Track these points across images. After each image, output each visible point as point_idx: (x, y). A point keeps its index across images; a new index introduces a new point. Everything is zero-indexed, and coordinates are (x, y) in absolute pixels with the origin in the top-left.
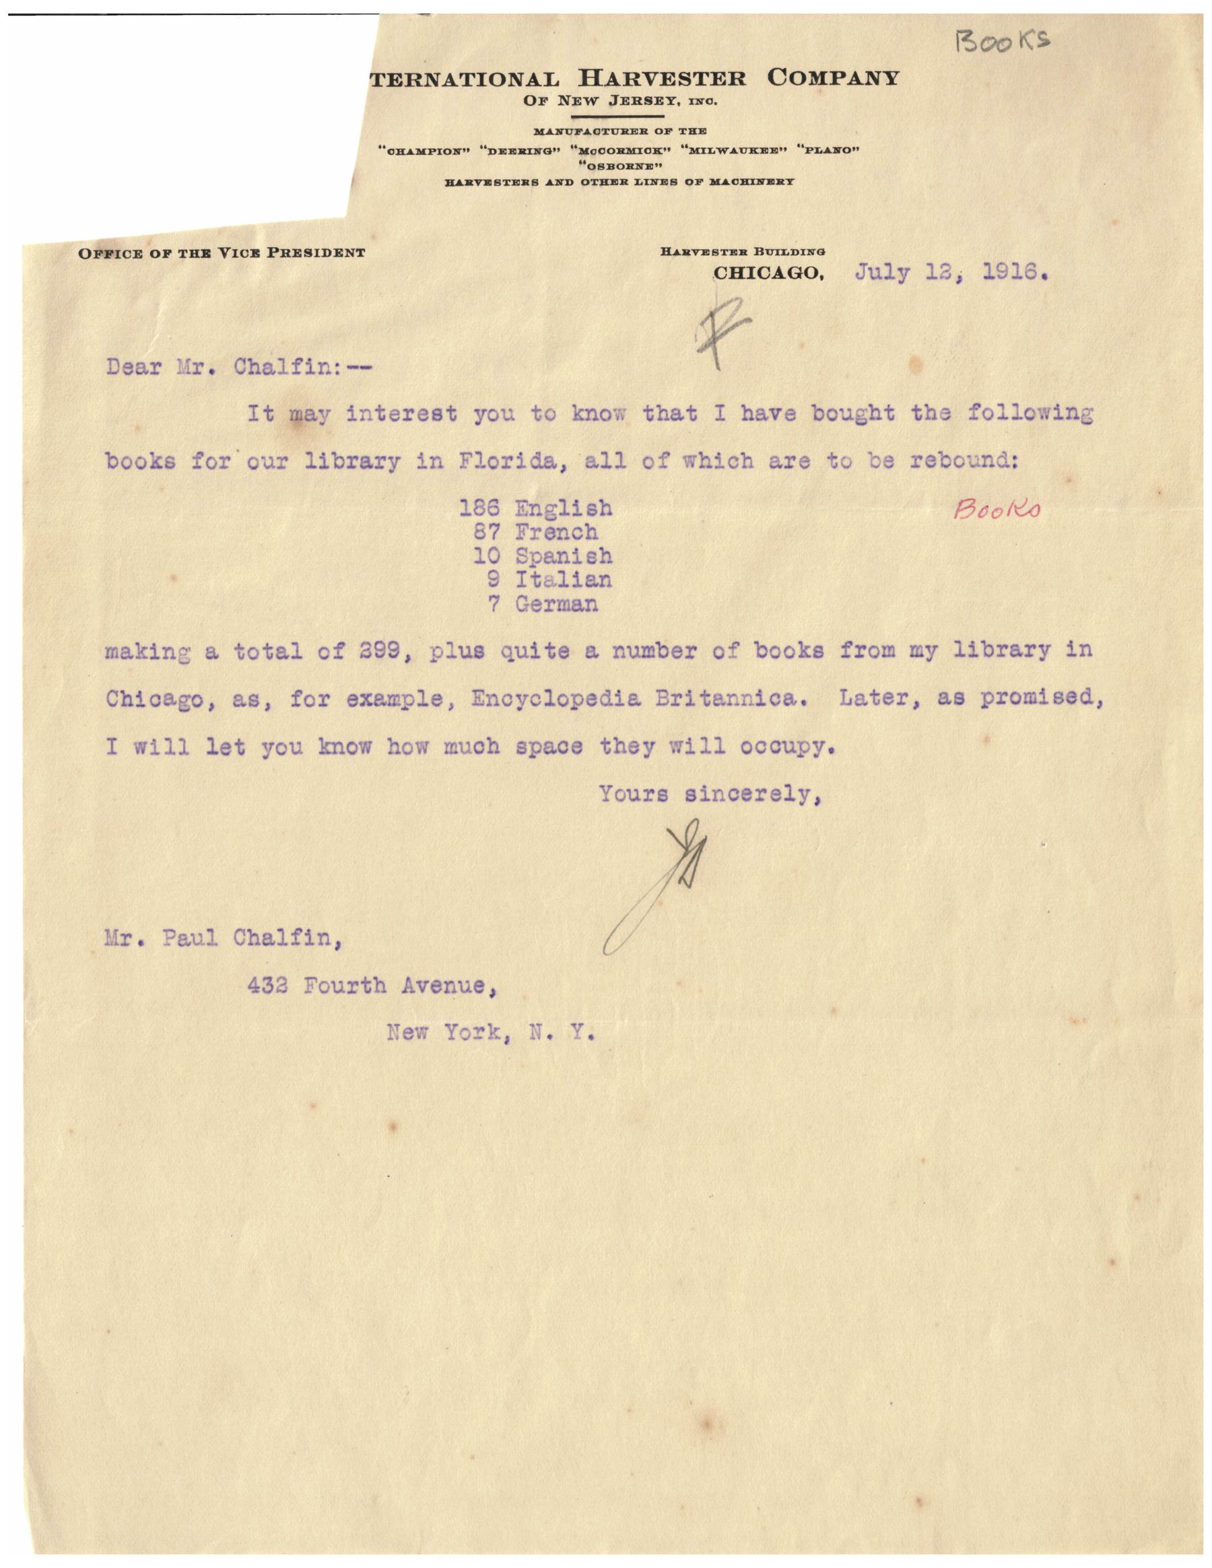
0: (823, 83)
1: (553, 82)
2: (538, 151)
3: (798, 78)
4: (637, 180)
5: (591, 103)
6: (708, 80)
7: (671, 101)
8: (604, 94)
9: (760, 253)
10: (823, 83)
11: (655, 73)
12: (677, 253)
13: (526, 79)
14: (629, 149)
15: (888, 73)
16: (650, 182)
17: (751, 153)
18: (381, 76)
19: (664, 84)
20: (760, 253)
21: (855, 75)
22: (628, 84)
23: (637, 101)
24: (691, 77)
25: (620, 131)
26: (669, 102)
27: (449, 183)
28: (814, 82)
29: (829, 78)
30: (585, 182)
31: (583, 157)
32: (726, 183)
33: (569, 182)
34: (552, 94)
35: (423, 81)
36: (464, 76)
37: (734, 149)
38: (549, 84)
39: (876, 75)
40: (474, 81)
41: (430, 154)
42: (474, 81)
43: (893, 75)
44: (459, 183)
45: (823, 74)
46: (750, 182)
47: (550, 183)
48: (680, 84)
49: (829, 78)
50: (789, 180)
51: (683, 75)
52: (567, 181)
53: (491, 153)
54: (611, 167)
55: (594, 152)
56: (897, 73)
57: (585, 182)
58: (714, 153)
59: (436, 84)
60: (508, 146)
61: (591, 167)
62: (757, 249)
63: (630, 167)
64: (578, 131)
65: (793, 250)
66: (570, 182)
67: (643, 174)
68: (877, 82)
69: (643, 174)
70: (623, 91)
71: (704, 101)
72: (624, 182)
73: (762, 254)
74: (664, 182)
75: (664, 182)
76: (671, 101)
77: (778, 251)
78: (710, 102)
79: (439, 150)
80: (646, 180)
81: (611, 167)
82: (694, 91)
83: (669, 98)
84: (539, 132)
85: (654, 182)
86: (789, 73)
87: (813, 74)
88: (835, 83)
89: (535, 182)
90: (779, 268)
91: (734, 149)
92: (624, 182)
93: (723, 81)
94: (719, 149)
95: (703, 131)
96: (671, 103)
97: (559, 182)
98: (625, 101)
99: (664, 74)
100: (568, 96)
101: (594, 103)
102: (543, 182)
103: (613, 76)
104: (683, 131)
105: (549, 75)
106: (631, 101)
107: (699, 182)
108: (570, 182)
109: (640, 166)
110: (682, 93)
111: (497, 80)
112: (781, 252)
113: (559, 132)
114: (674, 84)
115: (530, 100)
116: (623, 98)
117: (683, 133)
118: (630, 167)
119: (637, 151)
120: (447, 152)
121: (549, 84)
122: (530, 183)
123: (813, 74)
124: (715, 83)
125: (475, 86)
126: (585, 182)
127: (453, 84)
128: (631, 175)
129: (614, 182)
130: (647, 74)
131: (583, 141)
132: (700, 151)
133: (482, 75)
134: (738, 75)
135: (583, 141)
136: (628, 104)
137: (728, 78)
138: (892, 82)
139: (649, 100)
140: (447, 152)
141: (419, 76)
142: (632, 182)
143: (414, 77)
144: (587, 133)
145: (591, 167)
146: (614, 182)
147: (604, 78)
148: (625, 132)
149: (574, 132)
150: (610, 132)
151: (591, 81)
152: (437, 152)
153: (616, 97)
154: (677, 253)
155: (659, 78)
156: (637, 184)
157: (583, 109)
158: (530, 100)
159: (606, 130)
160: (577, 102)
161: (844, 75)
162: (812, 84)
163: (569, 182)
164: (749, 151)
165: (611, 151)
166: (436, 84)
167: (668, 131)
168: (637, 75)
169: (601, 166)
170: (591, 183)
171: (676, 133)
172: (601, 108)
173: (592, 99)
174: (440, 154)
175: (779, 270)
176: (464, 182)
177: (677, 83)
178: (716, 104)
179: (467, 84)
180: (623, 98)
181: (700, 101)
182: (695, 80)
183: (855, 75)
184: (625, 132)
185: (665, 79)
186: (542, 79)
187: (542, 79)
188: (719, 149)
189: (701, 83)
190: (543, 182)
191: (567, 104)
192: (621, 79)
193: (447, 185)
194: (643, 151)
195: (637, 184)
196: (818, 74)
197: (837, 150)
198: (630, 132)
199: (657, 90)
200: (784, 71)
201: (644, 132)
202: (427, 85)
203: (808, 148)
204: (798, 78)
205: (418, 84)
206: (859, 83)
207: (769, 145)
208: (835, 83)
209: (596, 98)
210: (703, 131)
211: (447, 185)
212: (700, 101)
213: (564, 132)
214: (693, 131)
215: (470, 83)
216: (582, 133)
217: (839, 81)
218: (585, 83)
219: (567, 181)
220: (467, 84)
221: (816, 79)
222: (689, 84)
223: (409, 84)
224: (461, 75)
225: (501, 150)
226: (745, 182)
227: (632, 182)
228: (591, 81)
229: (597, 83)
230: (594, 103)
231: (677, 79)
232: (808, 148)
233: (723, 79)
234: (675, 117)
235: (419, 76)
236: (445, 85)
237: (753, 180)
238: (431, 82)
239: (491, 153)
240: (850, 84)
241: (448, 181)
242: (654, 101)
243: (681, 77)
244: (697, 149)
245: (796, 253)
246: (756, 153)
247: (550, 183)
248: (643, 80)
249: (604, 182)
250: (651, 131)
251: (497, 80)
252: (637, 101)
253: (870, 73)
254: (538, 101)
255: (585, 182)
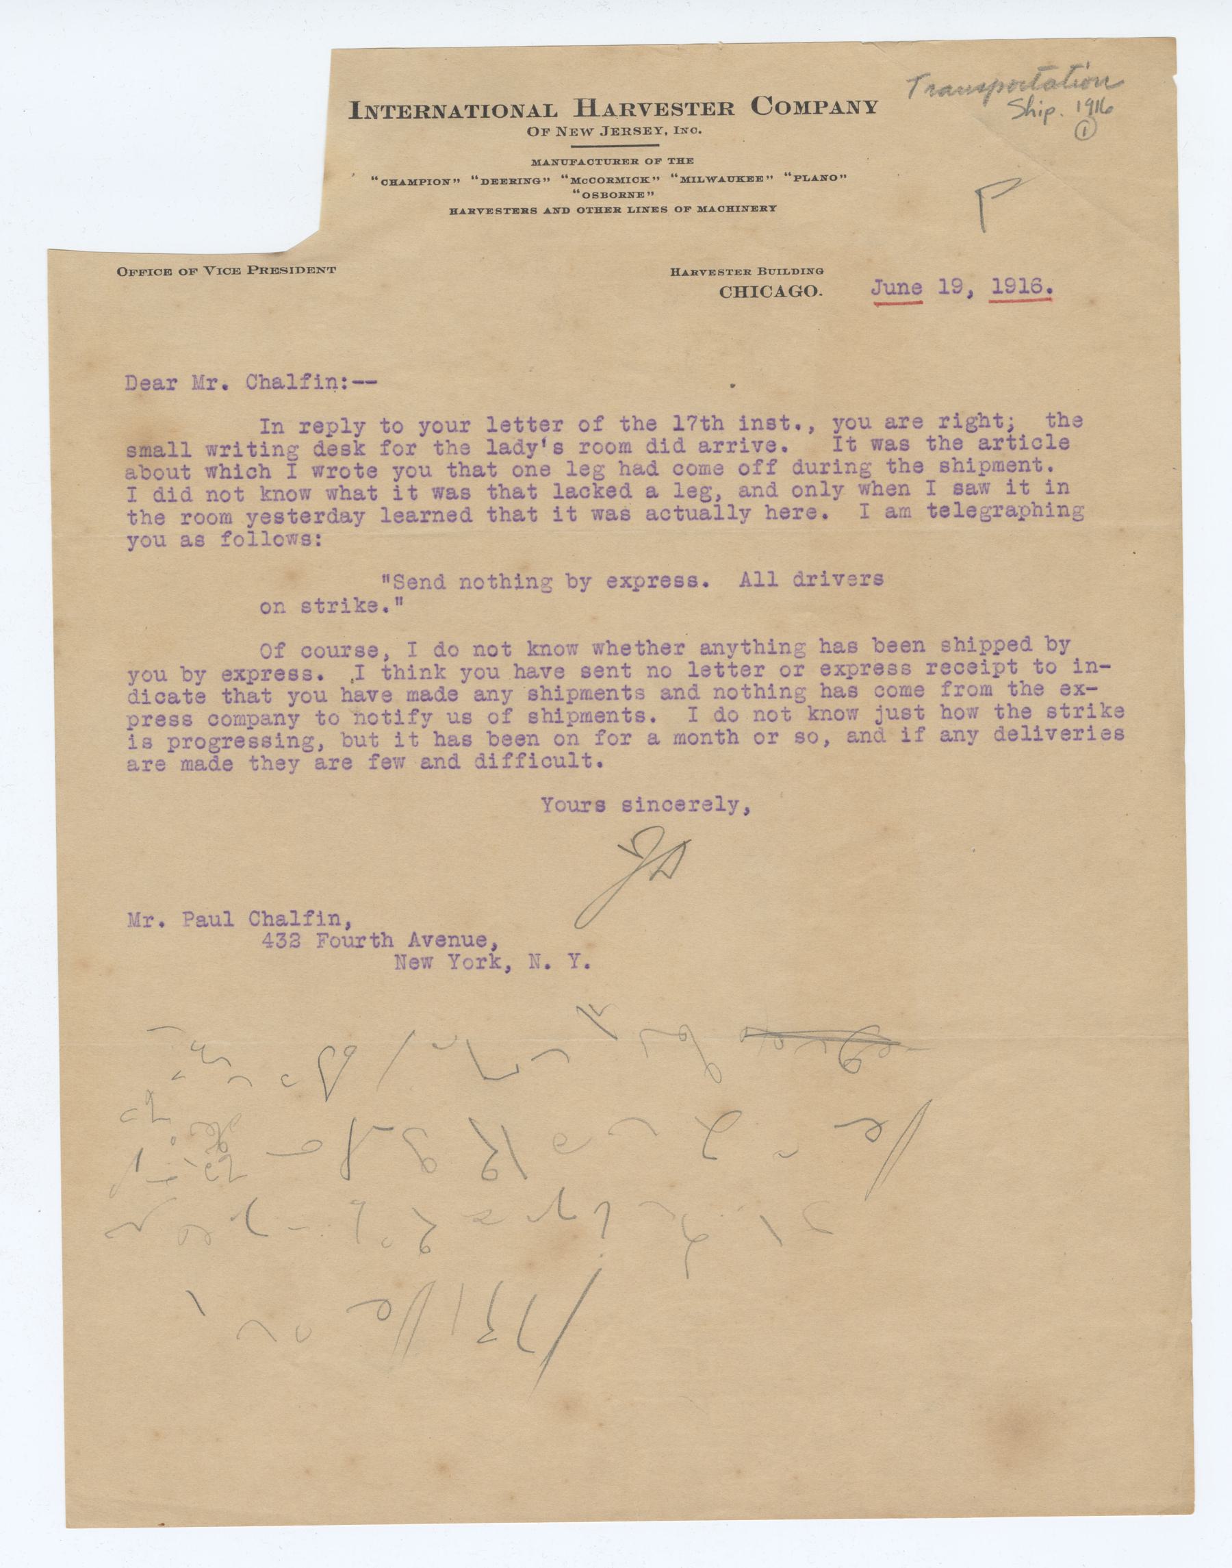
0: (807, 112)
1: (552, 113)
2: (527, 181)
3: (783, 108)
4: (630, 208)
5: (587, 133)
6: (699, 110)
7: (658, 131)
8: (597, 124)
9: (763, 273)
10: (807, 112)
11: (650, 104)
12: (685, 274)
13: (527, 110)
14: (618, 179)
15: (868, 103)
16: (641, 210)
17: (738, 181)
18: (391, 109)
19: (658, 114)
20: (763, 273)
21: (837, 104)
22: (623, 114)
23: (627, 132)
24: (683, 108)
25: (612, 162)
26: (656, 132)
27: (453, 212)
28: (799, 111)
29: (812, 108)
30: (581, 210)
31: (576, 187)
32: (712, 210)
33: (566, 211)
34: (550, 123)
35: (431, 113)
36: (469, 108)
37: (722, 178)
38: (548, 115)
39: (856, 104)
40: (478, 113)
41: (421, 184)
42: (478, 113)
43: (872, 104)
44: (463, 212)
45: (807, 104)
46: (735, 209)
47: (548, 211)
48: (673, 114)
49: (812, 108)
50: (771, 207)
51: (675, 105)
52: (564, 209)
53: (483, 184)
54: (604, 195)
55: (585, 181)
56: (876, 102)
57: (581, 210)
58: (703, 181)
59: (442, 115)
60: (499, 176)
61: (586, 195)
62: (760, 268)
63: (622, 195)
64: (573, 162)
65: (794, 270)
66: (566, 211)
67: (635, 202)
68: (857, 111)
69: (635, 202)
70: (612, 122)
71: (689, 131)
72: (617, 210)
73: (765, 273)
74: (655, 209)
75: (655, 209)
76: (658, 131)
77: (779, 270)
78: (694, 130)
79: (429, 180)
80: (638, 208)
81: (604, 195)
82: (684, 120)
83: (657, 128)
84: (536, 163)
85: (646, 209)
86: (774, 103)
87: (798, 103)
88: (818, 112)
89: (534, 211)
90: (780, 287)
91: (722, 178)
92: (617, 210)
93: (713, 111)
94: (708, 178)
95: (690, 161)
96: (658, 133)
97: (557, 210)
98: (615, 132)
99: (658, 105)
100: (565, 128)
101: (589, 134)
102: (541, 210)
103: (610, 107)
104: (671, 160)
105: (548, 106)
106: (621, 132)
107: (687, 209)
108: (566, 211)
109: (631, 195)
110: (668, 123)
111: (500, 111)
112: (782, 272)
113: (555, 162)
114: (667, 114)
115: (533, 132)
116: (613, 129)
117: (671, 163)
118: (622, 195)
119: (625, 180)
120: (437, 182)
121: (548, 115)
122: (529, 211)
123: (798, 103)
124: (705, 113)
125: (479, 117)
126: (580, 210)
127: (459, 116)
128: (623, 204)
129: (608, 210)
130: (642, 105)
131: (576, 171)
132: (691, 180)
133: (485, 107)
134: (727, 106)
135: (576, 171)
136: (618, 134)
137: (717, 109)
138: (871, 111)
139: (637, 131)
140: (437, 182)
141: (427, 108)
142: (624, 209)
143: (422, 109)
144: (582, 163)
145: (586, 195)
146: (608, 210)
147: (601, 108)
148: (616, 162)
149: (569, 162)
150: (602, 162)
151: (587, 111)
152: (427, 182)
153: (606, 128)
154: (685, 274)
155: (653, 109)
156: (630, 212)
157: (581, 140)
158: (533, 132)
159: (599, 160)
160: (573, 132)
161: (826, 104)
162: (796, 113)
163: (566, 211)
164: (736, 179)
165: (601, 180)
166: (442, 115)
167: (658, 161)
168: (633, 106)
169: (595, 195)
170: (587, 211)
171: (665, 162)
172: (595, 139)
173: (587, 130)
174: (429, 184)
175: (780, 289)
176: (467, 211)
177: (670, 113)
178: (700, 132)
179: (472, 116)
180: (613, 129)
181: (685, 131)
182: (687, 110)
183: (837, 104)
184: (616, 162)
185: (658, 110)
186: (542, 111)
187: (542, 111)
188: (708, 178)
189: (692, 113)
190: (541, 210)
191: (564, 134)
192: (617, 110)
193: (452, 214)
194: (631, 180)
195: (630, 212)
196: (802, 103)
197: (824, 178)
198: (621, 162)
199: (651, 120)
200: (770, 99)
201: (635, 162)
202: (435, 117)
203: (796, 176)
204: (783, 108)
205: (426, 116)
206: (840, 112)
207: (756, 174)
208: (818, 112)
209: (592, 129)
210: (690, 161)
211: (452, 214)
212: (685, 131)
213: (560, 162)
214: (681, 161)
215: (475, 115)
216: (576, 163)
217: (821, 110)
218: (580, 114)
219: (564, 209)
220: (472, 116)
221: (801, 108)
222: (682, 113)
223: (722, 113)
224: (466, 107)
225: (493, 180)
226: (730, 209)
227: (624, 209)
228: (587, 111)
229: (593, 114)
230: (589, 134)
231: (670, 109)
232: (796, 176)
233: (713, 109)
234: (669, 146)
235: (427, 108)
236: (451, 117)
237: (738, 207)
238: (438, 114)
239: (483, 184)
240: (832, 113)
241: (452, 210)
242: (643, 131)
243: (673, 107)
244: (688, 178)
245: (796, 271)
246: (743, 181)
247: (548, 211)
248: (637, 110)
249: (599, 210)
250: (641, 161)
251: (500, 111)
252: (627, 132)
253: (851, 102)
254: (541, 132)
255: (580, 210)
